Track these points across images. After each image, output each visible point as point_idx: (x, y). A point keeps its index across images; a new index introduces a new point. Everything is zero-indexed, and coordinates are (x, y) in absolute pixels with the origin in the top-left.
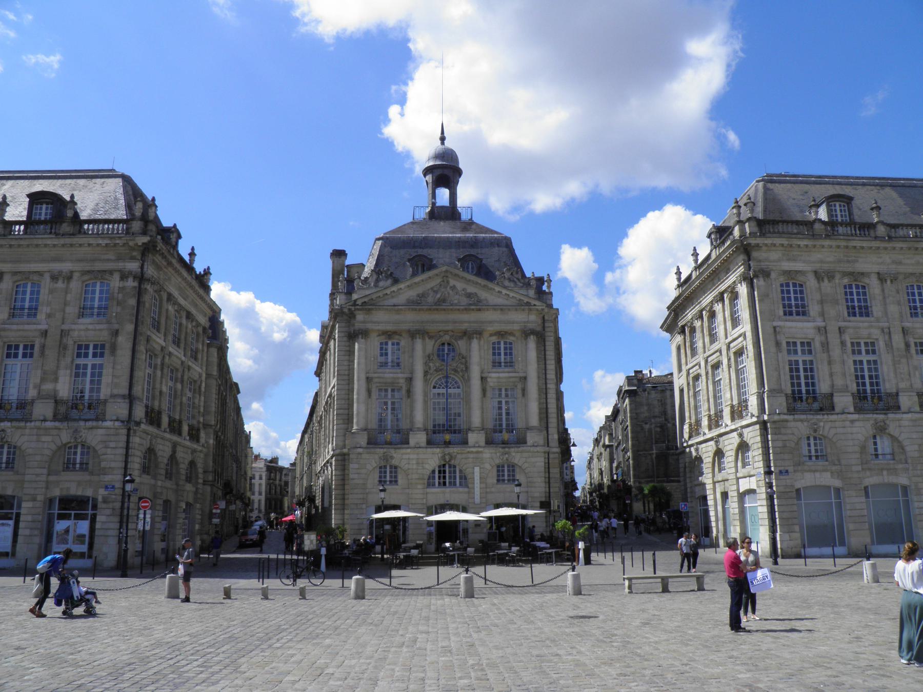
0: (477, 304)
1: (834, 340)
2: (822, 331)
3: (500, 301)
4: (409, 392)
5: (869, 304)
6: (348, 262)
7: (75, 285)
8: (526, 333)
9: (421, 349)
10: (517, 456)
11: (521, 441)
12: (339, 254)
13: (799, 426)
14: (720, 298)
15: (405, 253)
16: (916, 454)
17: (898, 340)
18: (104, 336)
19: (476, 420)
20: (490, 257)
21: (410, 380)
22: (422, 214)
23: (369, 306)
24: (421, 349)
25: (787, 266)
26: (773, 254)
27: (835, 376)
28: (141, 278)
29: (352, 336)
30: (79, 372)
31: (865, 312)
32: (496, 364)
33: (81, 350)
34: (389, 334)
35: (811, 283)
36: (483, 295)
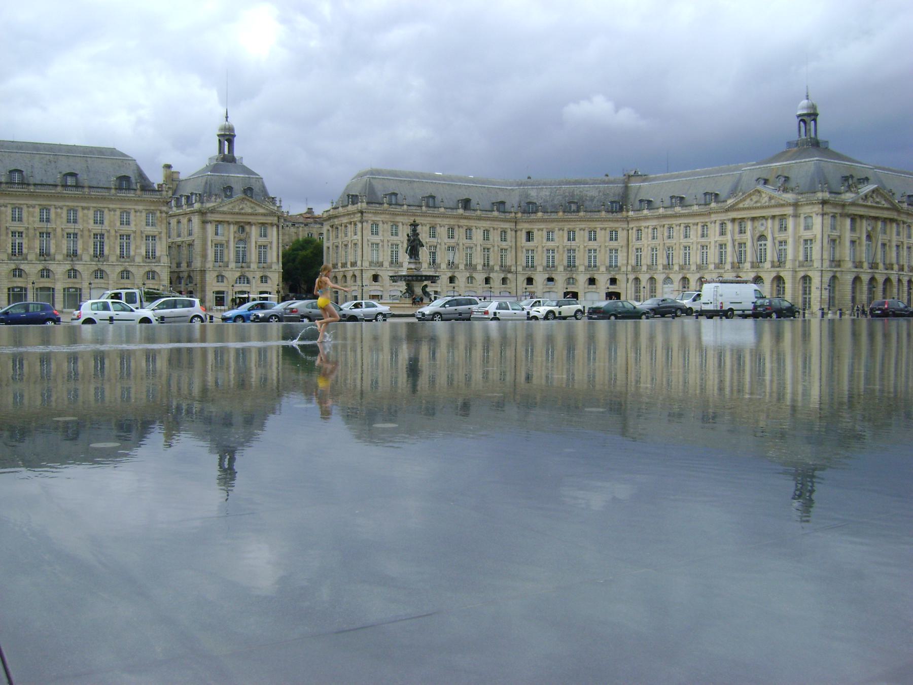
4: (228, 247)
6: (173, 170)
9: (233, 228)
14: (351, 223)
21: (228, 242)
24: (233, 228)
25: (374, 219)
34: (220, 222)
35: (381, 224)
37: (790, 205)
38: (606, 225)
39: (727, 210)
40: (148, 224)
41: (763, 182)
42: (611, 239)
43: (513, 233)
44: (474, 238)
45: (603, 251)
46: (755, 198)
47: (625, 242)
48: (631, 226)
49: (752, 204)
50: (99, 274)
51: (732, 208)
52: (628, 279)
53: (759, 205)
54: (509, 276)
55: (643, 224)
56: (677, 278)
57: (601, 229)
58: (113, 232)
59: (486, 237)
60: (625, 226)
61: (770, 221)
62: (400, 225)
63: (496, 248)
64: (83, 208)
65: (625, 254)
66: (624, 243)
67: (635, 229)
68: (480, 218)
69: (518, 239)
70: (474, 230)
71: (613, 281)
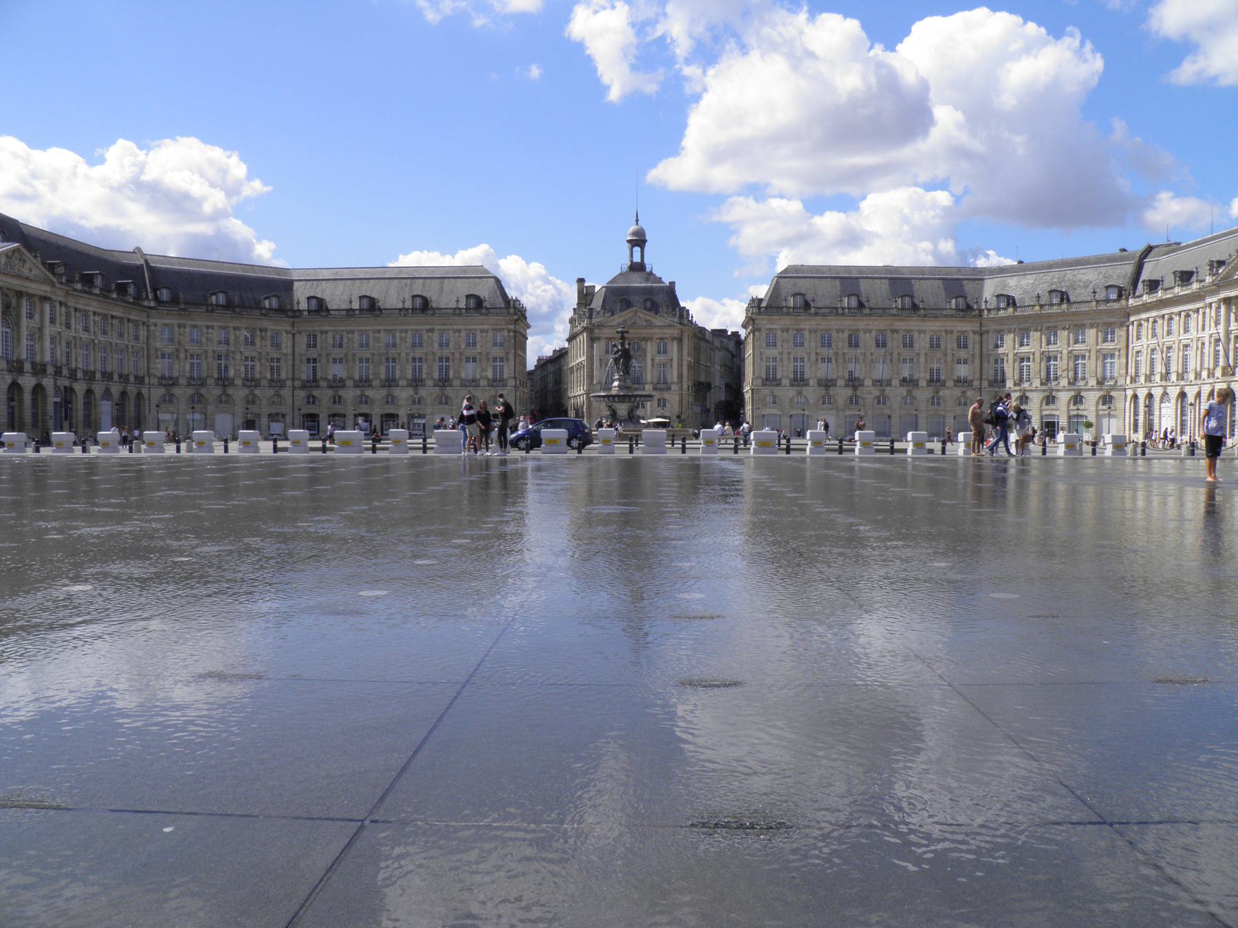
0: (650, 325)
1: (785, 358)
2: (781, 353)
3: (659, 323)
6: (586, 284)
7: (490, 334)
8: (673, 339)
10: (667, 395)
11: (669, 389)
12: (581, 281)
13: (766, 391)
15: (618, 296)
17: (813, 357)
18: (503, 355)
19: (649, 379)
20: (659, 299)
22: (625, 268)
23: (600, 326)
25: (769, 326)
26: (764, 322)
27: (785, 371)
28: (515, 332)
29: (592, 340)
30: (494, 368)
31: (802, 345)
32: (659, 352)
33: (495, 359)
35: (779, 333)
36: (653, 320)
40: (495, 344)
43: (977, 337)
44: (916, 345)
48: (1132, 319)
50: (444, 400)
54: (970, 393)
56: (1174, 392)
58: (457, 355)
59: (935, 345)
63: (949, 358)
64: (428, 331)
65: (1124, 360)
69: (984, 345)
70: (916, 335)
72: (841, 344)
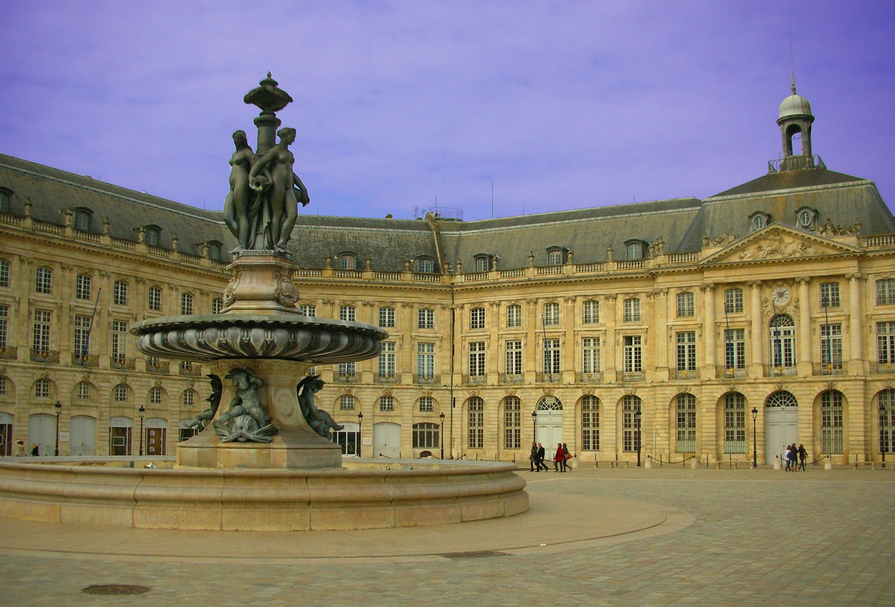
5: (9, 277)
16: (22, 393)
17: (24, 307)
37: (854, 257)
38: (413, 298)
39: (701, 270)
41: (765, 219)
42: (421, 325)
45: (406, 346)
46: (767, 246)
47: (448, 329)
49: (760, 256)
51: (714, 265)
52: (454, 401)
53: (779, 257)
55: (488, 298)
57: (404, 305)
60: (448, 302)
61: (803, 288)
62: (15, 261)
65: (448, 354)
66: (445, 332)
67: (467, 308)
68: (177, 269)
70: (166, 291)
71: (426, 403)
72: (67, 290)
